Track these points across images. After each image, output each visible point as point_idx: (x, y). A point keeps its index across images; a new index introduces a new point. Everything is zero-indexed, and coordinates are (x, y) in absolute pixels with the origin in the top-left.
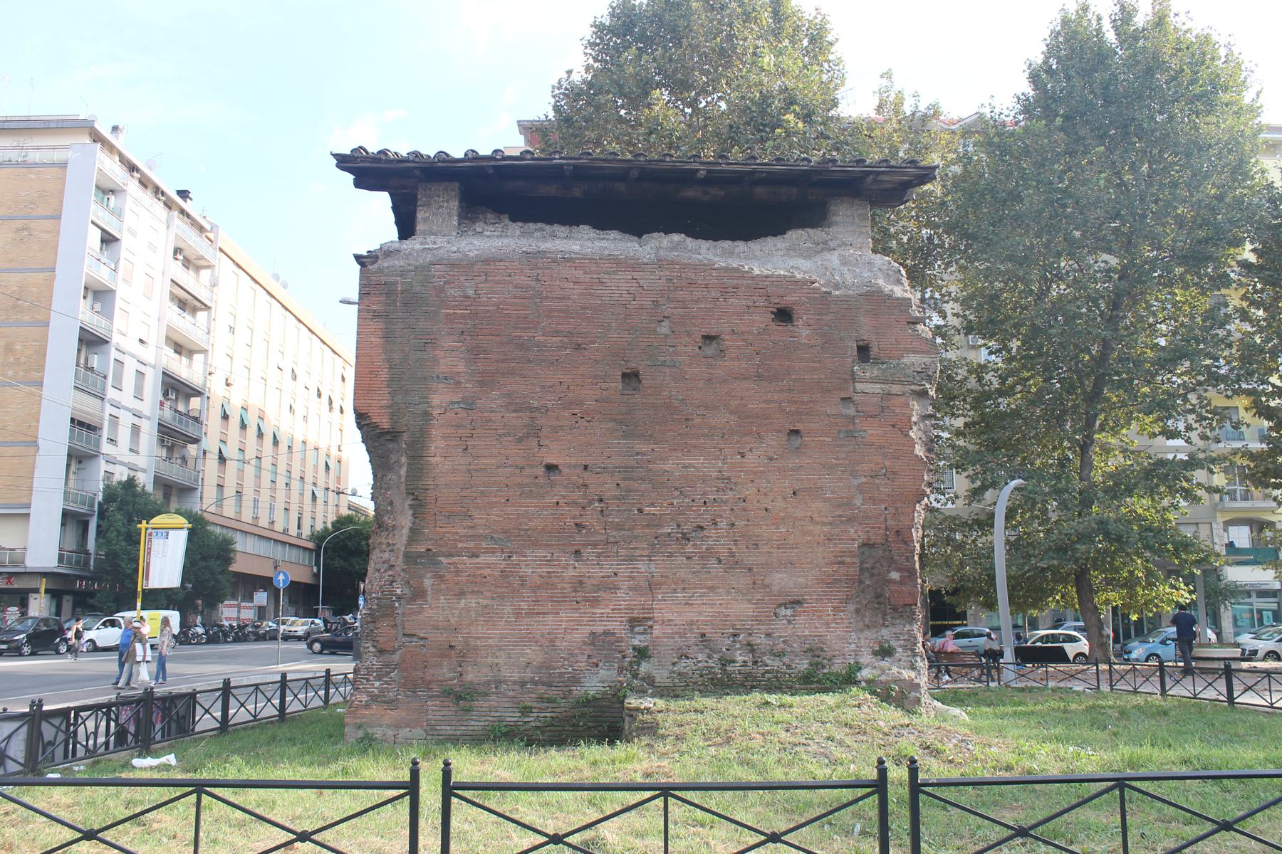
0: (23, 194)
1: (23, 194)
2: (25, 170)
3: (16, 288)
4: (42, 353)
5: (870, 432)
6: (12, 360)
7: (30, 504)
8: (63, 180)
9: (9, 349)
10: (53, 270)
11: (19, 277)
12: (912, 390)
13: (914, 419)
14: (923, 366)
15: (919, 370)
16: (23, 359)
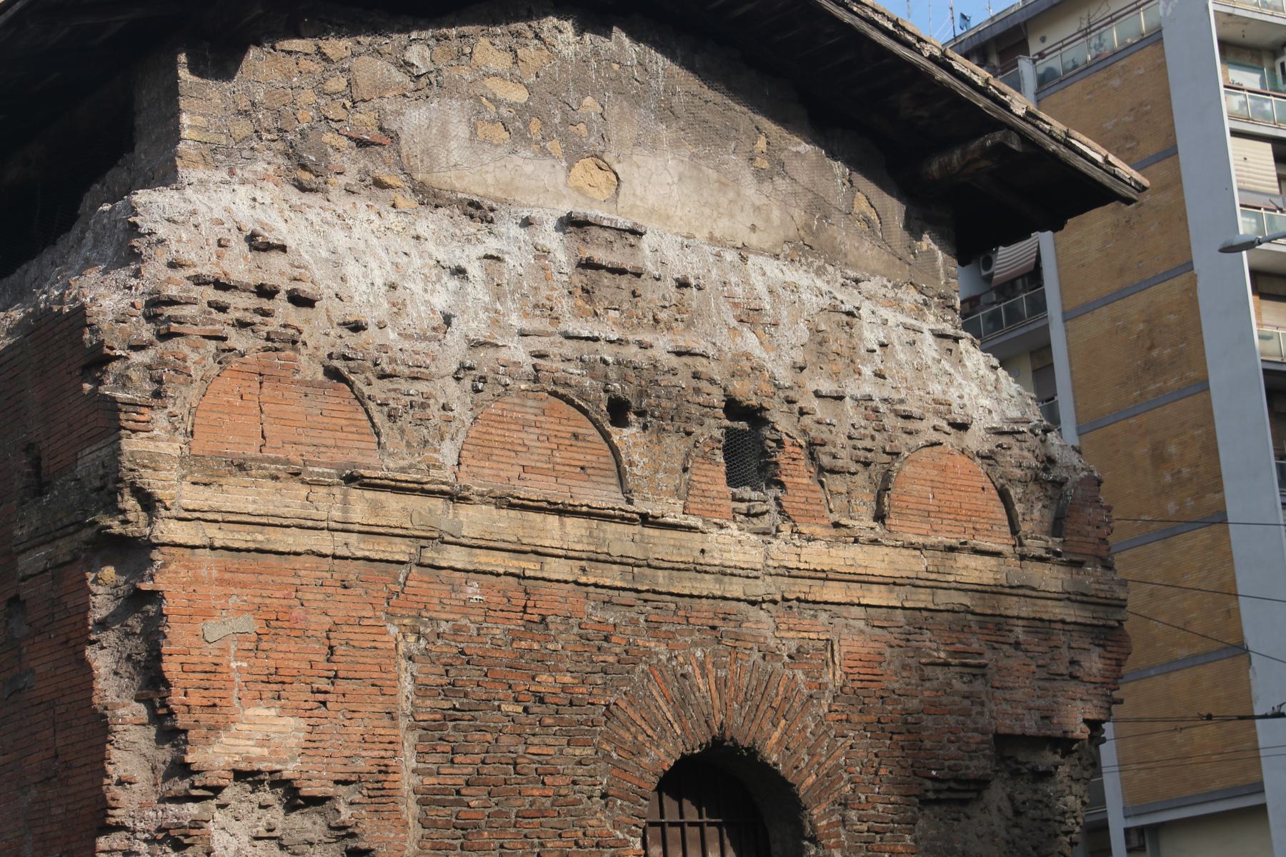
0: (1109, 125)
1: (1109, 125)
2: (1102, 75)
3: (1141, 326)
4: (1211, 449)
5: (38, 670)
6: (1168, 478)
7: (1261, 784)
8: (1161, 67)
9: (1159, 457)
10: (1189, 266)
11: (1140, 301)
12: (86, 543)
13: (98, 614)
14: (101, 472)
15: (97, 484)
16: (1186, 472)
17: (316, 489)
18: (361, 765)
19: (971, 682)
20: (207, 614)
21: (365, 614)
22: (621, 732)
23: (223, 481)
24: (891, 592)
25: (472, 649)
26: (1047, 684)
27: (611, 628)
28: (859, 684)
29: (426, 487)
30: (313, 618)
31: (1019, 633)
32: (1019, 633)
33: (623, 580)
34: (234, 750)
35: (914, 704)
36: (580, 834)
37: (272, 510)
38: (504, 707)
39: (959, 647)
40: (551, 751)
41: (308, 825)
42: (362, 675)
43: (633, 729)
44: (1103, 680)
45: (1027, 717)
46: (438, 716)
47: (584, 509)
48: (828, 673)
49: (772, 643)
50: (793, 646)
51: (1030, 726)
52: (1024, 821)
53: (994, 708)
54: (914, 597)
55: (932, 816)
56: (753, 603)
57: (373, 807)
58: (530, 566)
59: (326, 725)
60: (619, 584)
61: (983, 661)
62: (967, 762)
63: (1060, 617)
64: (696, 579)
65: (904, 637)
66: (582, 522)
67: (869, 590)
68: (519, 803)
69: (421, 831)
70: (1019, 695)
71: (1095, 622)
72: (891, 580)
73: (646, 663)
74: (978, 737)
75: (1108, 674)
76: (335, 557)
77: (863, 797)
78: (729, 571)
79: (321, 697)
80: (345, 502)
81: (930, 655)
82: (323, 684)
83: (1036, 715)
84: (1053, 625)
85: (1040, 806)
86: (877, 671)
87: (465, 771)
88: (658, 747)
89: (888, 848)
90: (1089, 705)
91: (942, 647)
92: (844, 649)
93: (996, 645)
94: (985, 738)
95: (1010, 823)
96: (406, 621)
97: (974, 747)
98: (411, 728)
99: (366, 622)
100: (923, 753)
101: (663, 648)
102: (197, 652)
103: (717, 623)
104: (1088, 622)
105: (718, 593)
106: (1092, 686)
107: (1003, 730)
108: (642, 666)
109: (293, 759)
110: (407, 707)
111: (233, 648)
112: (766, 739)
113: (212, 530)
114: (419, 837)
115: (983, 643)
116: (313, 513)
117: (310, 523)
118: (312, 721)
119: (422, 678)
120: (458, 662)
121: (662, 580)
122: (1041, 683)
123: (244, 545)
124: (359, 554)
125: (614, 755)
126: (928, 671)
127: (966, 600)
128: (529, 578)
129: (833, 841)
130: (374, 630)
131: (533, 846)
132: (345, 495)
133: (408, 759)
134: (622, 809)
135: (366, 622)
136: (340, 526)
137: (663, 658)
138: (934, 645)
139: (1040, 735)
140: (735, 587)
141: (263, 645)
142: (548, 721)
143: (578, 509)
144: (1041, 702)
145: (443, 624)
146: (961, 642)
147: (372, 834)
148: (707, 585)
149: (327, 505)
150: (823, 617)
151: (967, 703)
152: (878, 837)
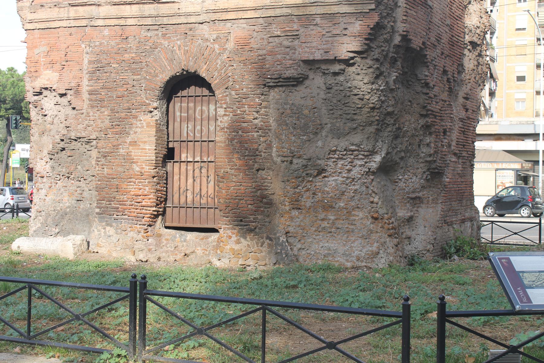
17: (61, 9)
18: (73, 84)
19: (292, 41)
20: (36, 47)
21: (75, 42)
22: (151, 70)
23: (38, 11)
24: (256, 12)
25: (105, 49)
26: (330, 39)
27: (149, 38)
28: (241, 47)
29: (87, 3)
30: (62, 45)
31: (318, 20)
32: (318, 20)
33: (153, 22)
34: (41, 82)
35: (264, 52)
36: (135, 102)
37: (49, 17)
38: (113, 65)
39: (287, 29)
40: (127, 77)
41: (64, 100)
42: (74, 60)
43: (154, 69)
44: (359, 34)
45: (317, 52)
46: (94, 70)
47: (135, 2)
48: (229, 44)
49: (206, 36)
50: (215, 37)
51: (318, 56)
52: (332, 91)
53: (301, 50)
54: (266, 13)
55: (278, 91)
56: (202, 23)
57: (75, 96)
58: (122, 22)
59: (64, 74)
60: (150, 24)
61: (297, 33)
62: (285, 72)
63: (336, 12)
64: (178, 18)
65: (263, 28)
66: (137, 6)
67: (247, 13)
68: (116, 93)
69: (89, 102)
70: (314, 44)
71: (356, 11)
72: (255, 8)
73: (160, 48)
74: (291, 62)
75: (362, 32)
76: (69, 27)
77: (238, 86)
78: (188, 14)
79: (63, 67)
80: (68, 11)
81: (273, 33)
82: (64, 63)
83: (322, 51)
84: (335, 15)
85: (338, 85)
86: (247, 42)
87: (101, 85)
88: (163, 74)
89: (247, 104)
90: (350, 45)
91: (279, 30)
92: (235, 35)
93: (305, 26)
94: (294, 62)
95: (325, 92)
96: (87, 43)
97: (288, 66)
98: (87, 74)
99: (76, 44)
100: (264, 70)
101: (166, 42)
102: (33, 57)
103: (186, 32)
104: (352, 12)
105: (186, 22)
106: (354, 37)
107: (304, 59)
108: (159, 49)
109: (55, 84)
110: (85, 68)
111: (42, 55)
112: (201, 69)
113: (36, 24)
114: (88, 104)
115: (298, 26)
116: (60, 16)
117: (59, 19)
118: (60, 73)
119: (90, 59)
120: (100, 53)
121: (165, 21)
122: (327, 39)
123: (44, 28)
124: (73, 26)
125: (148, 77)
126: (271, 40)
127: (289, 11)
128: (122, 26)
129: (223, 102)
130: (78, 47)
131: (120, 106)
132: (68, 9)
133: (85, 82)
134: (149, 94)
135: (76, 44)
136: (67, 18)
137: (166, 45)
138: (276, 30)
139: (322, 59)
140: (192, 19)
141: (49, 54)
142: (126, 69)
143: (133, 2)
144: (325, 46)
145: (97, 43)
146: (288, 27)
147: (76, 103)
148: (183, 20)
149: (63, 13)
150: (229, 24)
151: (289, 49)
152: (244, 100)
